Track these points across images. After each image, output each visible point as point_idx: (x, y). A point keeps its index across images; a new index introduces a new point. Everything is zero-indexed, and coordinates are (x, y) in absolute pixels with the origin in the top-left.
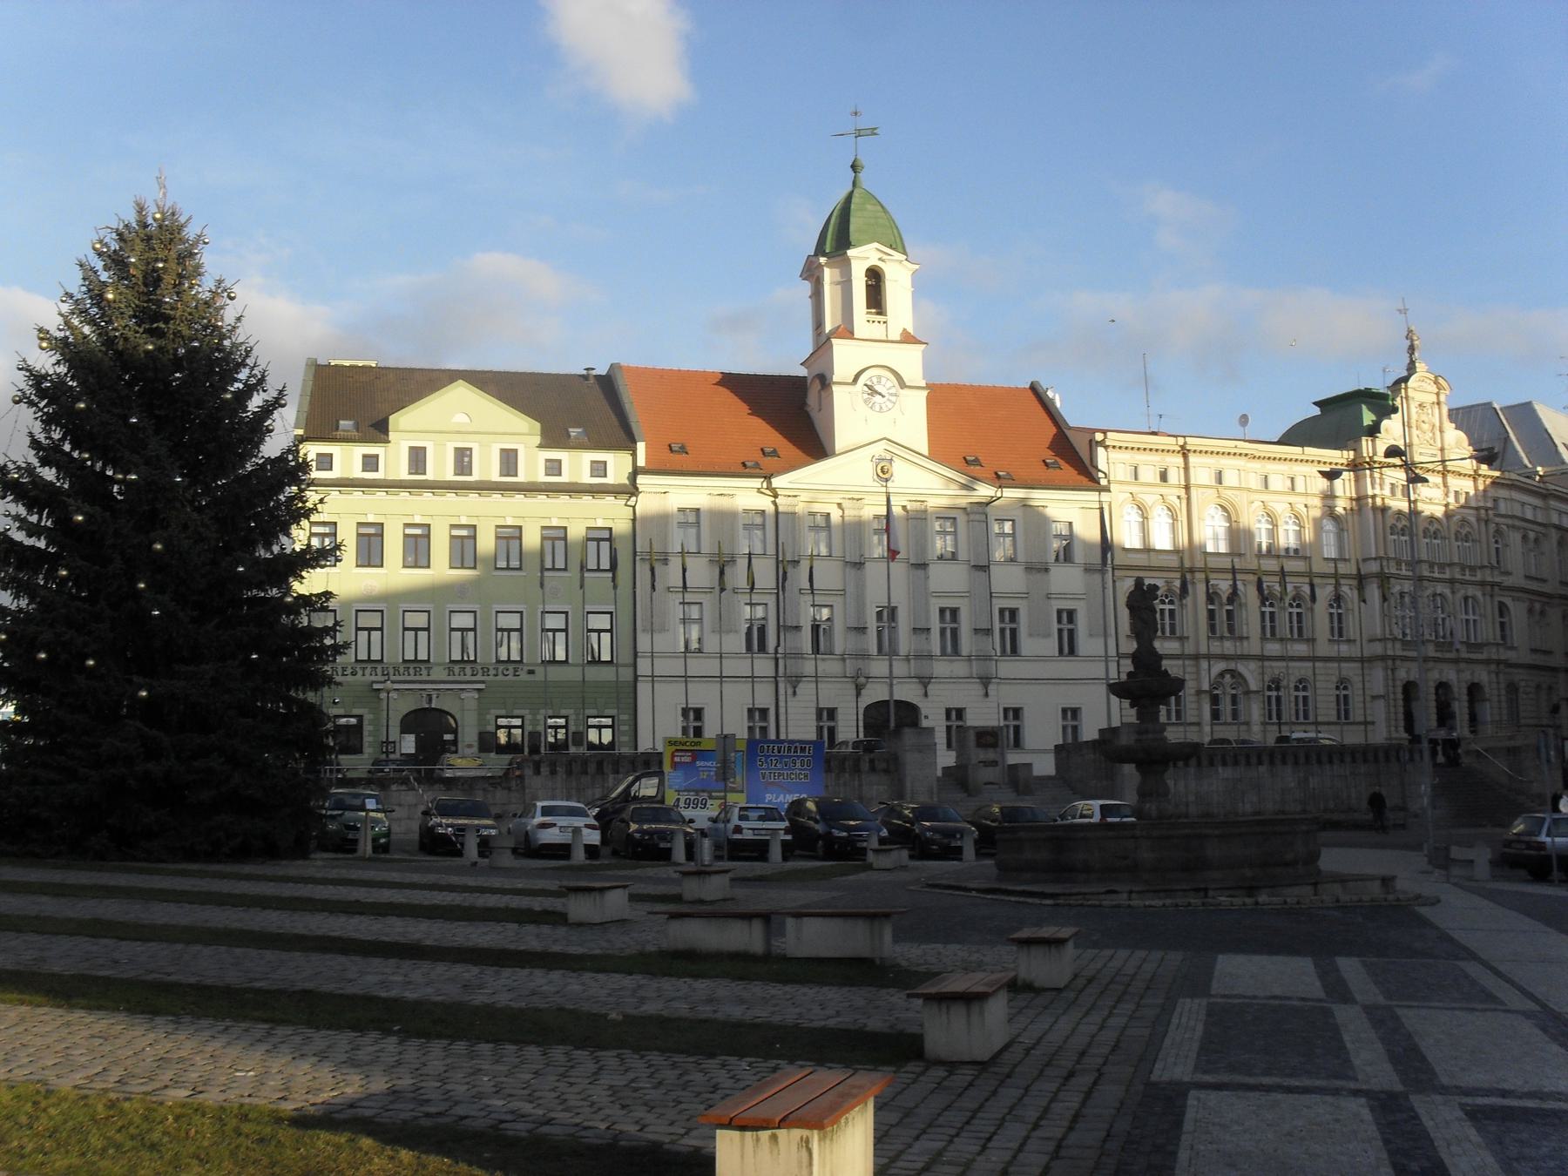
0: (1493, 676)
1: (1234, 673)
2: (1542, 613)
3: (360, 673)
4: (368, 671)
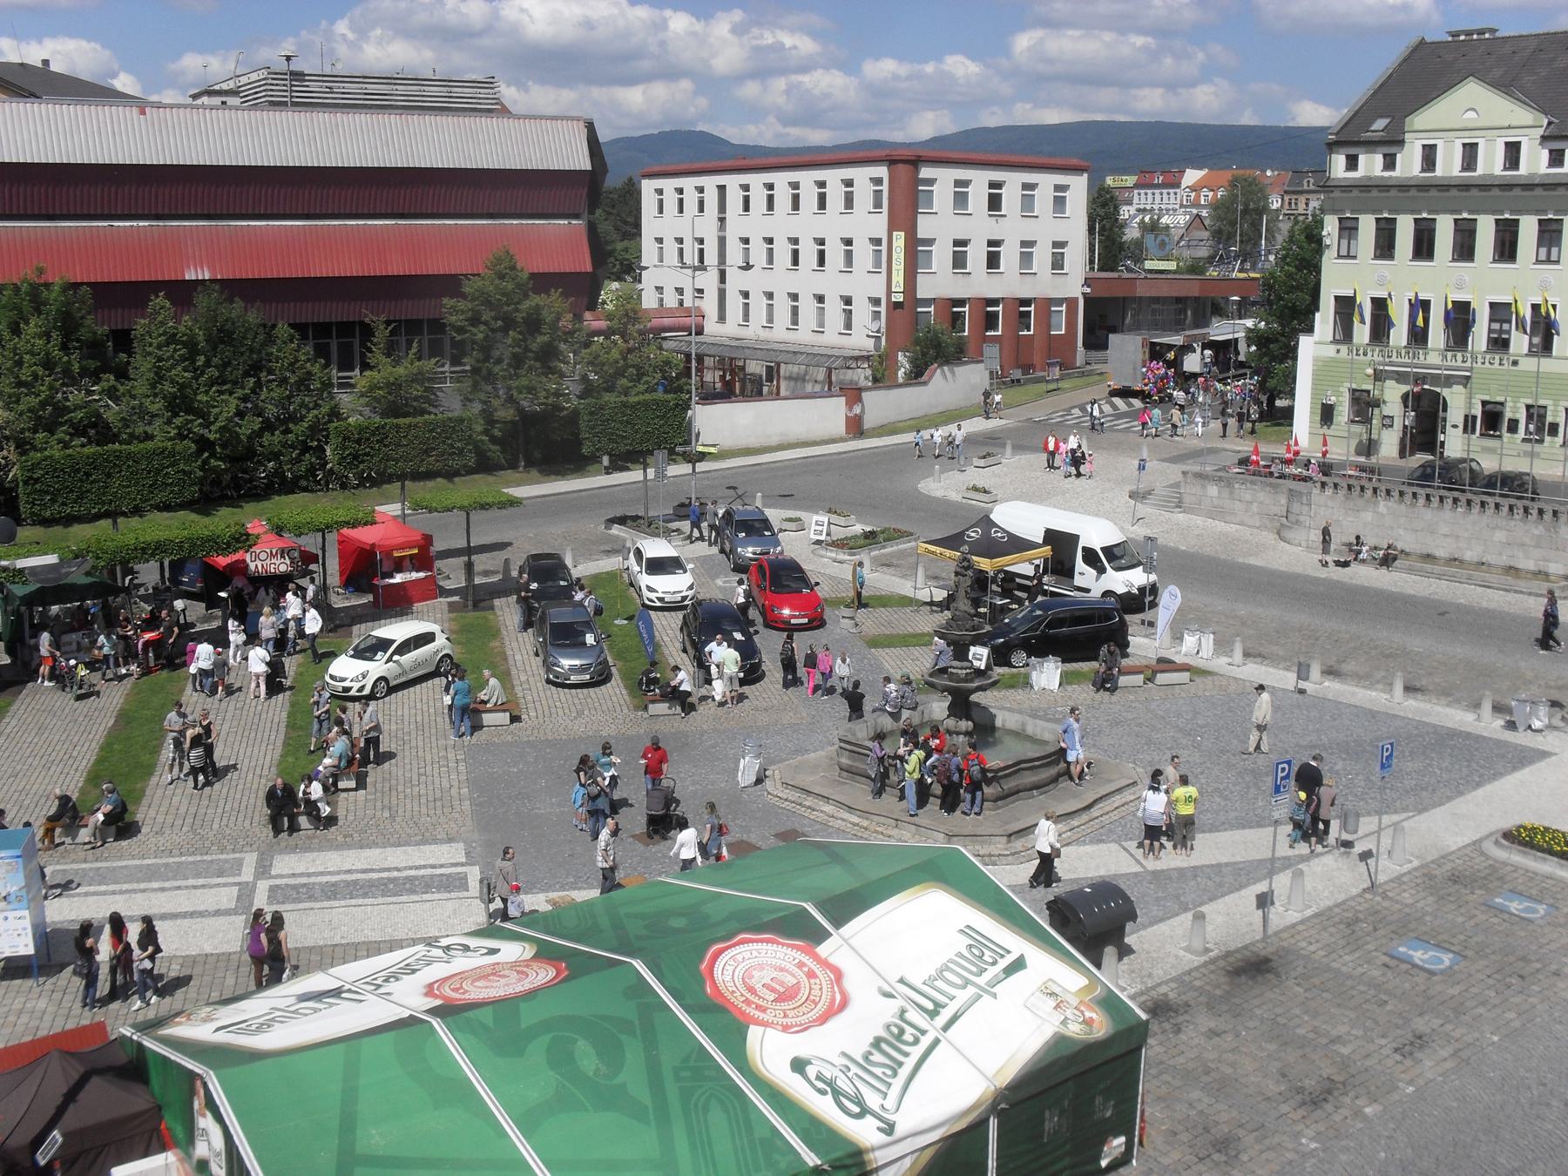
3: (1370, 354)
4: (1376, 354)
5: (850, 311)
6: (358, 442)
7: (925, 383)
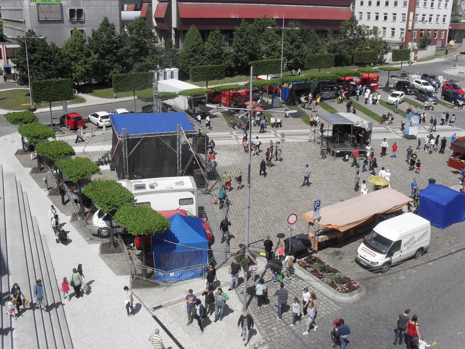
5: (394, 32)
6: (360, 56)
7: (426, 50)
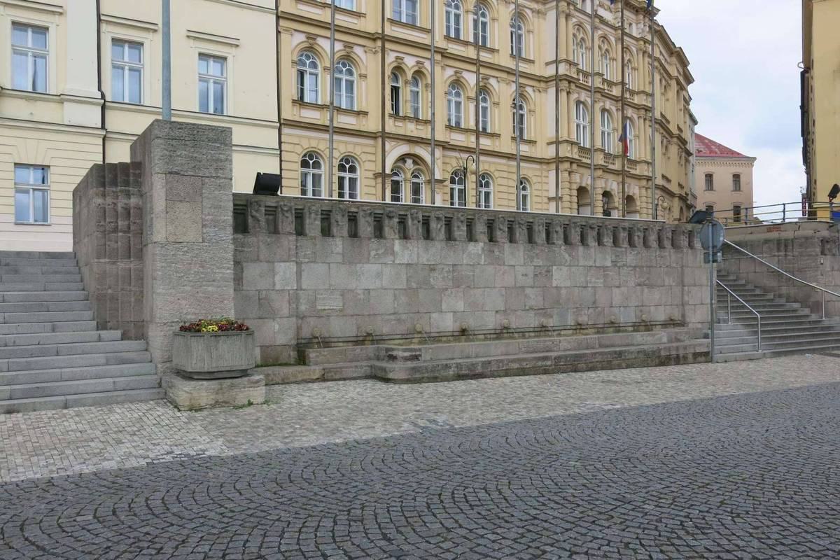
0: (644, 191)
1: (417, 159)
2: (666, 147)
